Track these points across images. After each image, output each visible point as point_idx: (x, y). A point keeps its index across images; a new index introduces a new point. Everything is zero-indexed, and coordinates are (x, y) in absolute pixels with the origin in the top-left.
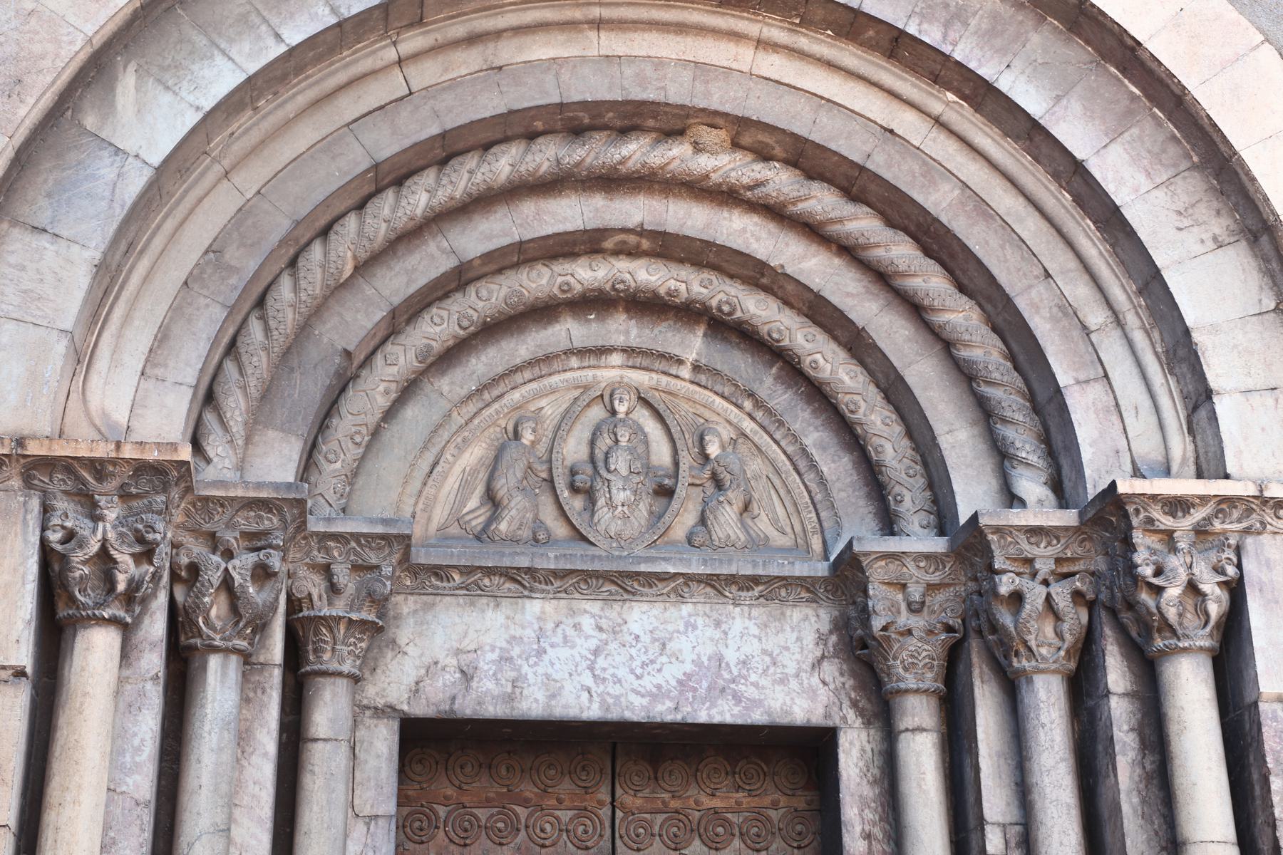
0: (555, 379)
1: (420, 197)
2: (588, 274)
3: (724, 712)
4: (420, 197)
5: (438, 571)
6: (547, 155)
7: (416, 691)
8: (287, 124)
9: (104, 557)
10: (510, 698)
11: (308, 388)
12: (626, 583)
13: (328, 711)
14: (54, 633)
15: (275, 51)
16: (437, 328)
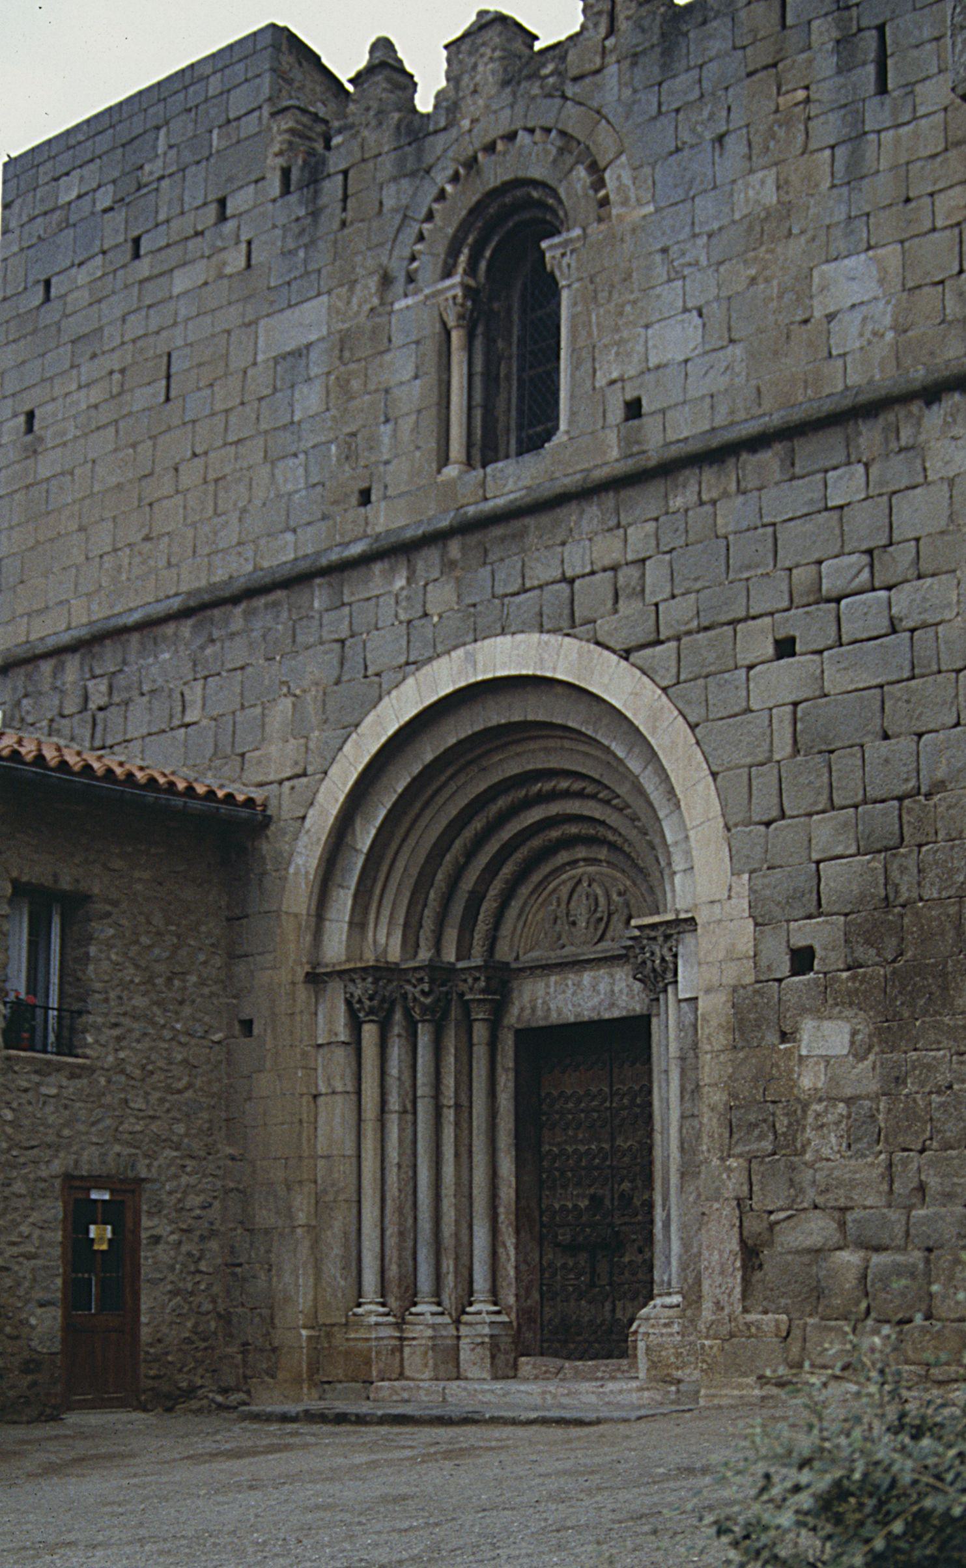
0: (564, 877)
1: (478, 824)
5: (521, 970)
7: (519, 1018)
8: (418, 816)
9: (360, 1001)
10: (546, 1018)
12: (578, 964)
13: (480, 1032)
14: (356, 1026)
15: (394, 797)
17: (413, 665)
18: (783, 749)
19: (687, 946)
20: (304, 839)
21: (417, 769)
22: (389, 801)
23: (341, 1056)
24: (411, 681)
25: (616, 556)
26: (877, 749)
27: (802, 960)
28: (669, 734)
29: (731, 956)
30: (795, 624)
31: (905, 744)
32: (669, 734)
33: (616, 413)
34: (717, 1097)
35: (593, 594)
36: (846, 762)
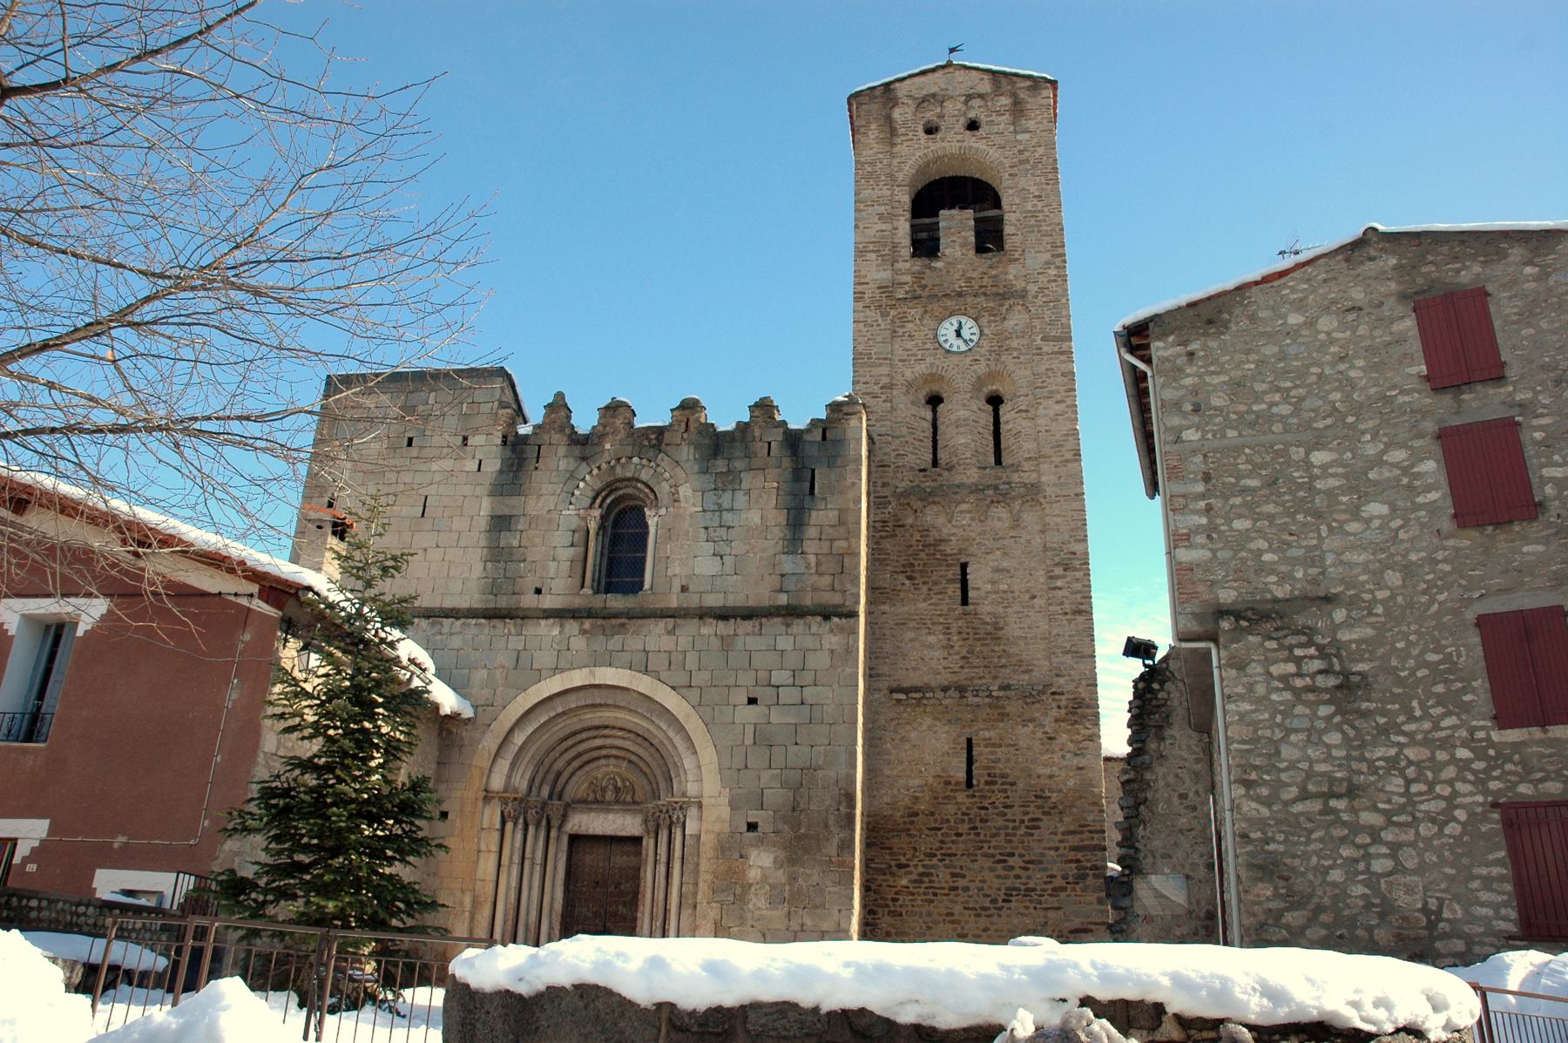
2: (604, 752)
3: (624, 834)
4: (569, 742)
6: (591, 733)
11: (551, 777)
13: (553, 833)
14: (503, 822)
16: (576, 764)
17: (556, 670)
18: (749, 741)
19: (693, 812)
20: (489, 734)
21: (552, 714)
22: (536, 725)
23: (497, 835)
24: (558, 677)
25: (672, 647)
26: (792, 749)
27: (752, 827)
28: (694, 726)
29: (718, 819)
30: (757, 692)
31: (807, 749)
32: (694, 726)
33: (676, 587)
34: (708, 877)
35: (656, 662)
36: (778, 752)
